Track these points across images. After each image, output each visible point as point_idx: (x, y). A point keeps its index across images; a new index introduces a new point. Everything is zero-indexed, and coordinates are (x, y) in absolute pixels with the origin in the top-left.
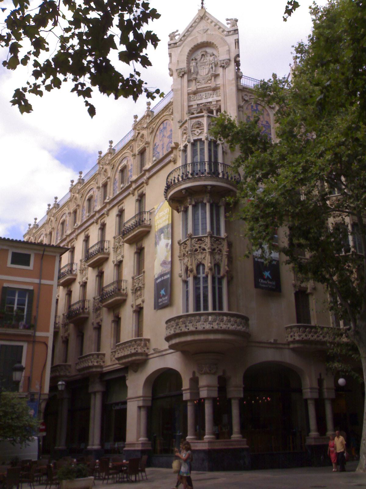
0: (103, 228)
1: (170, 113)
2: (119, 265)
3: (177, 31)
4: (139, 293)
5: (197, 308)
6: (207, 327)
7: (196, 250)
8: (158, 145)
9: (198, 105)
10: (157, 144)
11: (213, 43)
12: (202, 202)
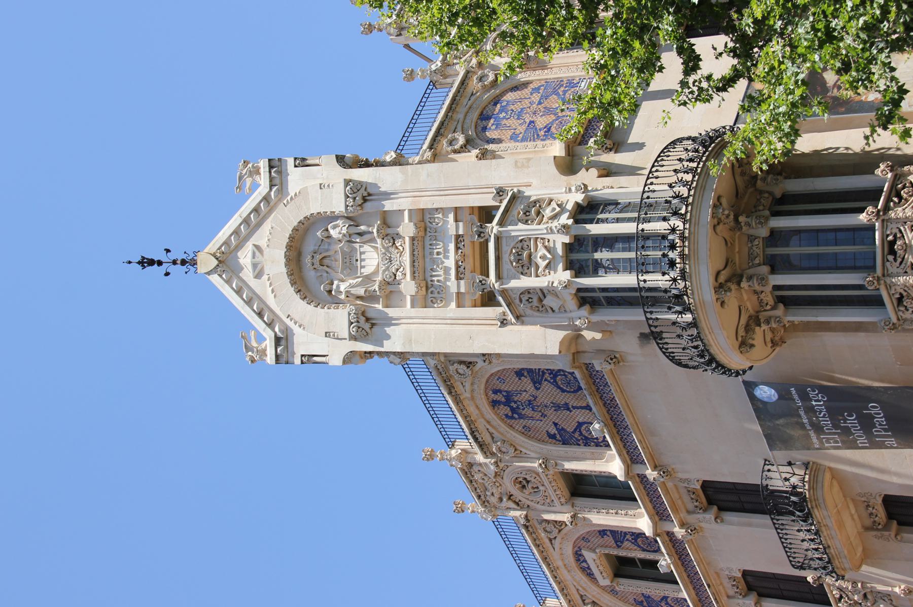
1: (468, 372)
8: (556, 424)
9: (458, 278)
10: (553, 431)
11: (295, 230)
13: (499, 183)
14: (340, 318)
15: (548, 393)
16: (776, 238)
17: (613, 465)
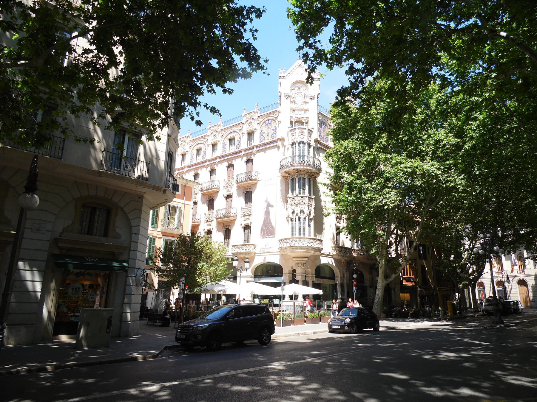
5: (300, 234)
14: (288, 91)
15: (271, 132)
16: (304, 179)
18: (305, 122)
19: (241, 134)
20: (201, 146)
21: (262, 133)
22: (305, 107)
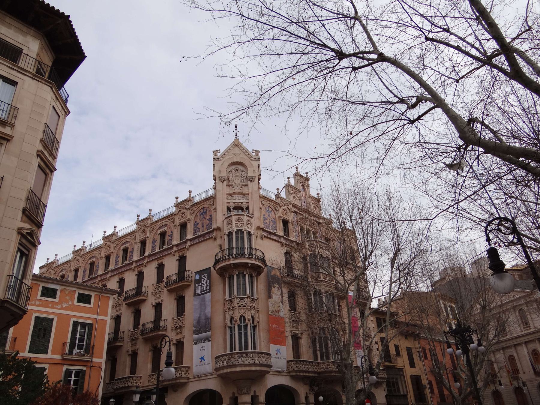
0: (140, 276)
2: (158, 307)
3: (219, 150)
4: (179, 330)
6: (251, 362)
7: (239, 306)
12: (243, 273)
13: (255, 214)
17: (189, 236)
18: (245, 208)
19: (172, 227)
20: (128, 245)
21: (195, 225)
22: (245, 190)
